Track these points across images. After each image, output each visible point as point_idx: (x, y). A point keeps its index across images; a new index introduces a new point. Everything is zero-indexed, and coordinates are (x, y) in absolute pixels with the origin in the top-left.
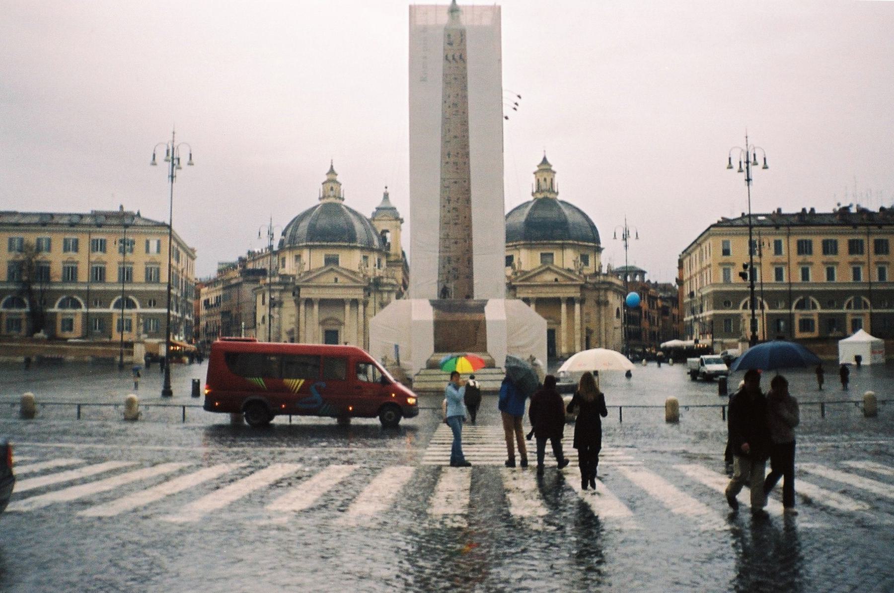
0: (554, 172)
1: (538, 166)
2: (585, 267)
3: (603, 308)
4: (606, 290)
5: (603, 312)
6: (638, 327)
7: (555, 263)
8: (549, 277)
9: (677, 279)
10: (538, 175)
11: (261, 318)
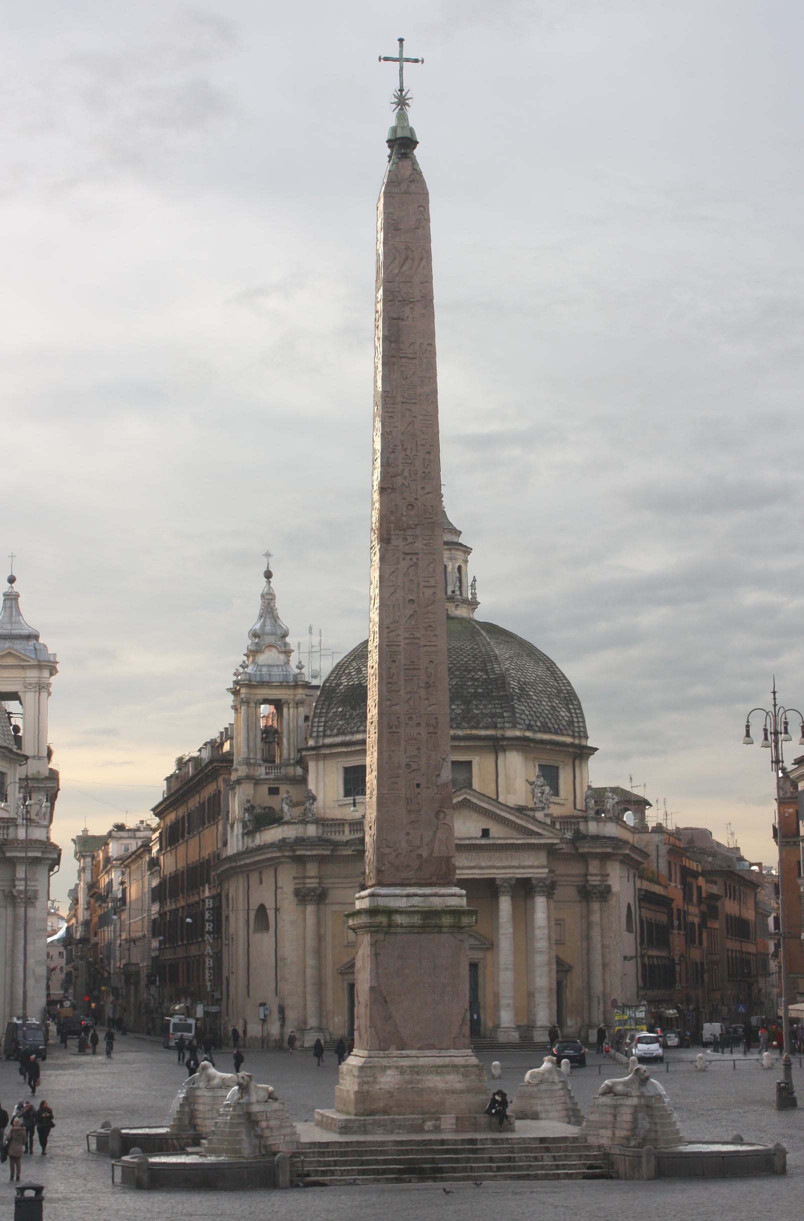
0: (467, 550)
2: (554, 799)
3: (596, 906)
4: (605, 858)
5: (596, 918)
7: (475, 786)
9: (774, 827)
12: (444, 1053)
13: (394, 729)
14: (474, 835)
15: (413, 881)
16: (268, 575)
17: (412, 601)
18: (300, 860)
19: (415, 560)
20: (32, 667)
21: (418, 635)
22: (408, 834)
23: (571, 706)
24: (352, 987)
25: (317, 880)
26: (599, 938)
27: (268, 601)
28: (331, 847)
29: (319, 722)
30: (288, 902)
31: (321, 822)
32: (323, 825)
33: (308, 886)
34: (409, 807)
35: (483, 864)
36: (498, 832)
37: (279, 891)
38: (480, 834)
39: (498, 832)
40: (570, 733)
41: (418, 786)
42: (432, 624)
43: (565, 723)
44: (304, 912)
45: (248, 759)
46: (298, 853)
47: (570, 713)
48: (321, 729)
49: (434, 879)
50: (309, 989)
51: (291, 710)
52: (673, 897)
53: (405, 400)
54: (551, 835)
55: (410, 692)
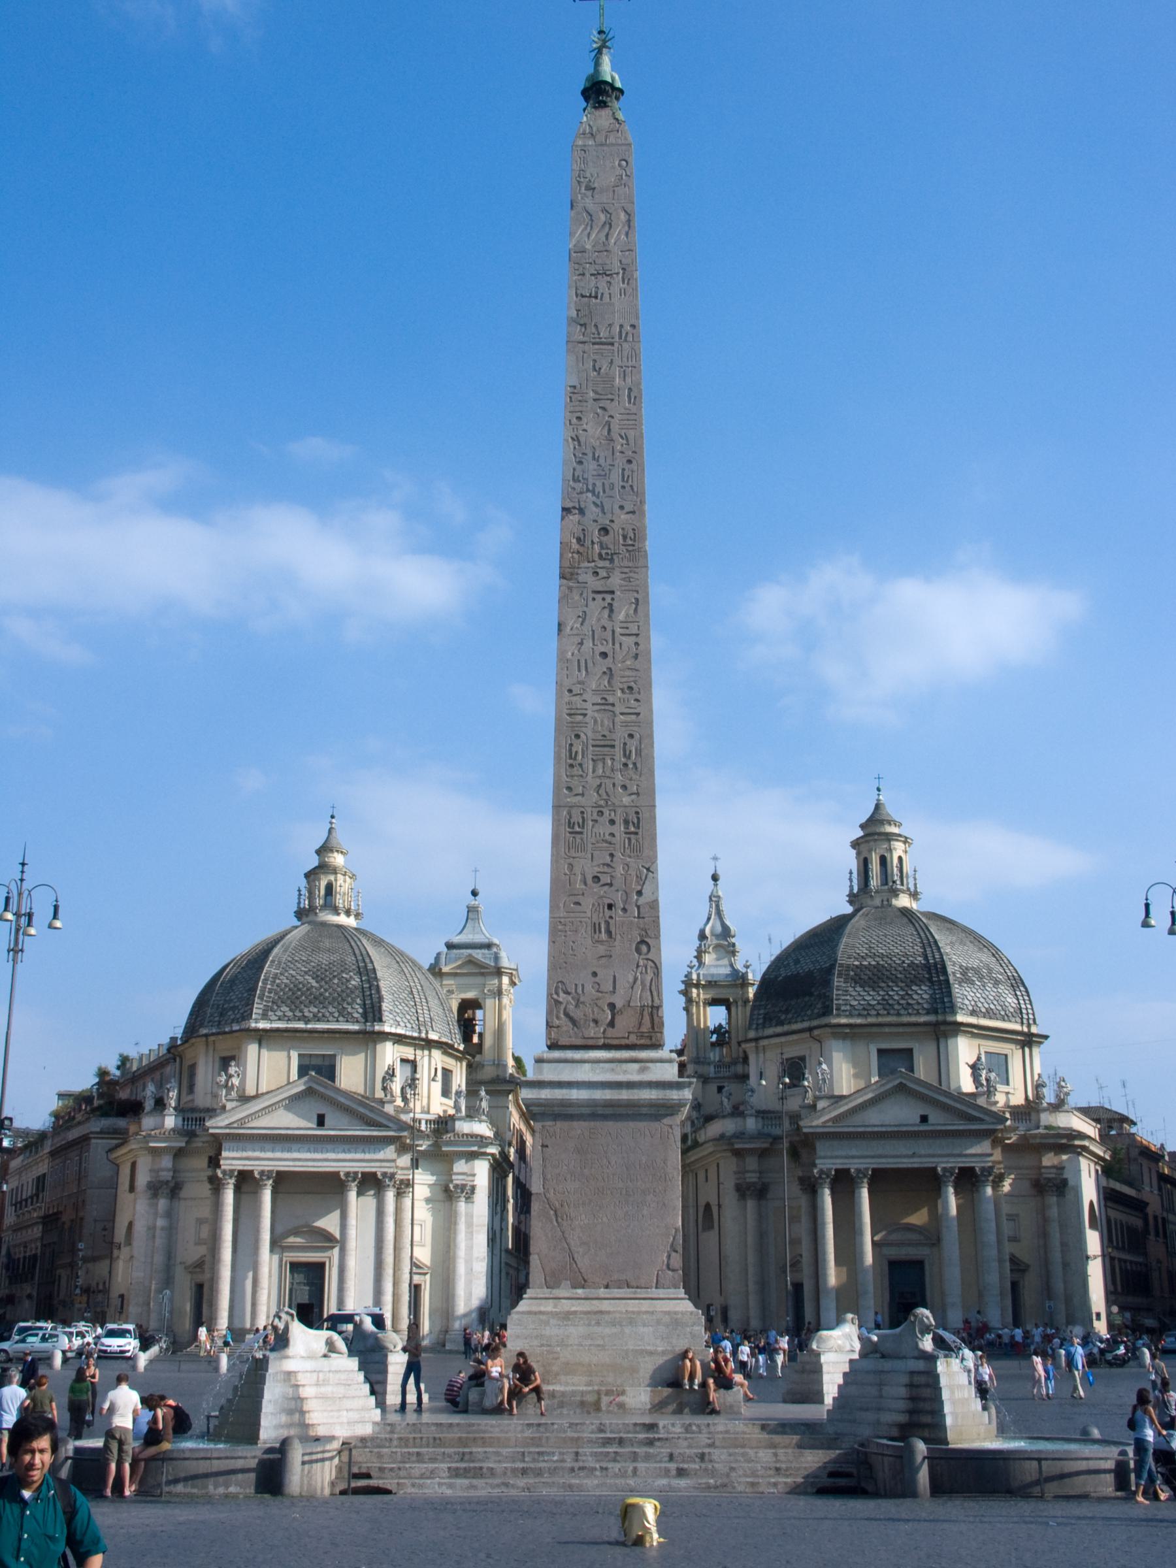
1: (862, 826)
5: (1054, 1212)
6: (1141, 1259)
8: (901, 1114)
10: (864, 847)
11: (126, 1224)
12: (641, 1293)
13: (577, 829)
14: (911, 1122)
15: (601, 1042)
16: (715, 878)
17: (604, 655)
18: (738, 1153)
19: (608, 600)
20: (491, 974)
21: (611, 699)
22: (595, 974)
23: (1018, 993)
24: (798, 1287)
25: (758, 1175)
26: (1058, 1235)
27: (715, 900)
28: (771, 1140)
29: (759, 1014)
30: (730, 1199)
31: (762, 1114)
32: (763, 1118)
33: (748, 1180)
34: (596, 936)
35: (923, 1152)
36: (937, 1120)
37: (721, 1186)
38: (918, 1120)
39: (937, 1120)
40: (1018, 1020)
41: (610, 906)
42: (632, 684)
43: (1012, 1010)
44: (745, 1208)
45: (698, 1058)
46: (737, 1146)
47: (1018, 999)
48: (761, 1021)
49: (633, 1039)
50: (752, 1287)
51: (740, 1008)
52: (1147, 1201)
53: (597, 397)
54: (995, 1121)
55: (599, 777)
